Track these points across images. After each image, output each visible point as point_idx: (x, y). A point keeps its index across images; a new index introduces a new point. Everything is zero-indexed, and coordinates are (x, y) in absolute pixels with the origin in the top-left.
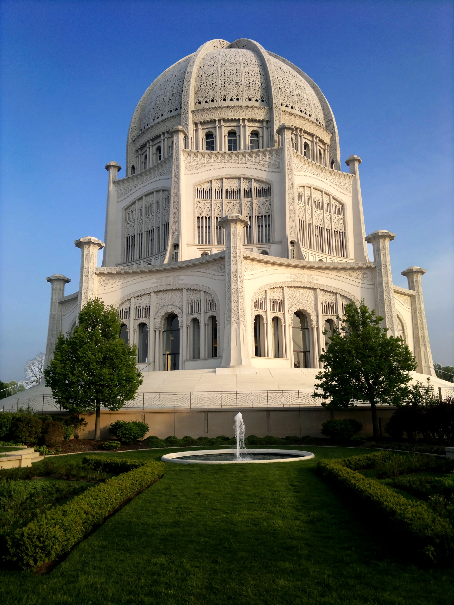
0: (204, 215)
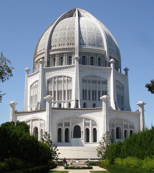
0: (85, 89)
